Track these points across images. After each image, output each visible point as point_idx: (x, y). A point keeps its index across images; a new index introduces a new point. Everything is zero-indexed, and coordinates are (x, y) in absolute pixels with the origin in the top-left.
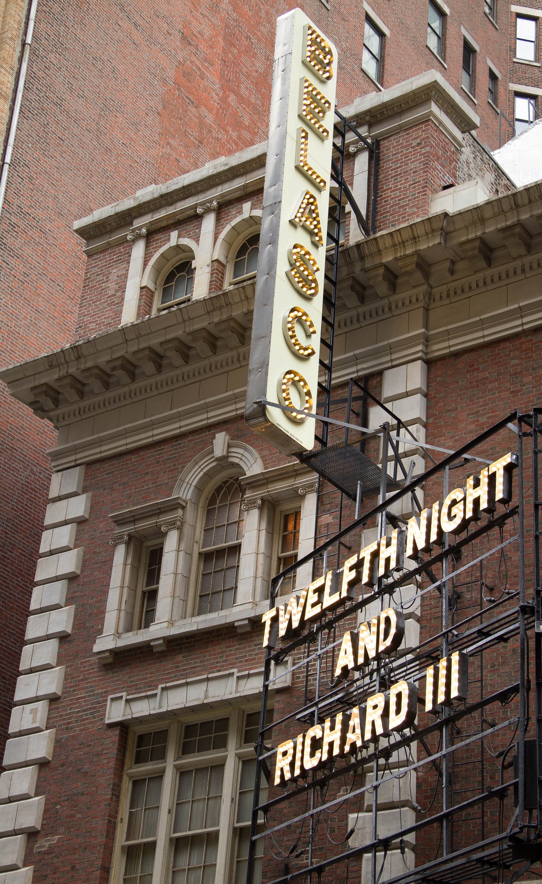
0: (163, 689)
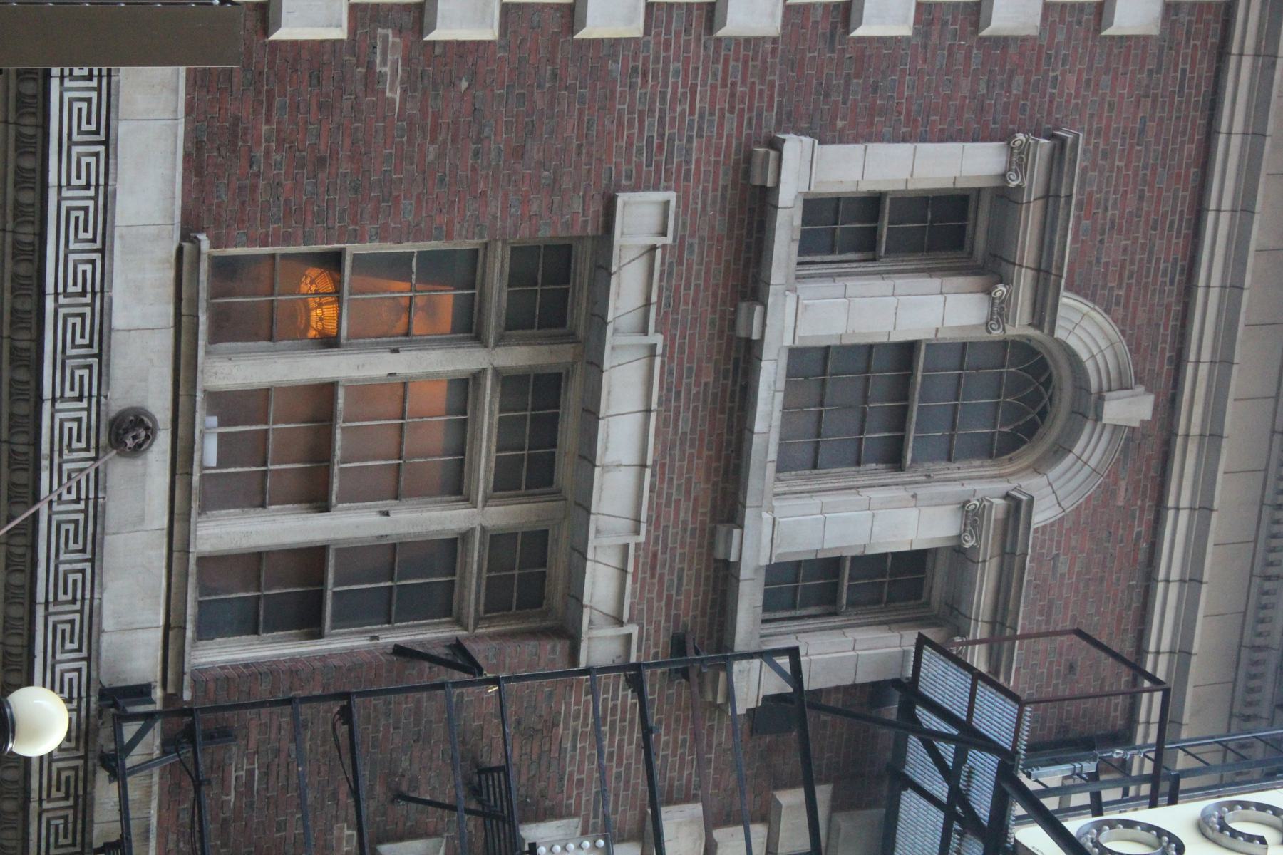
0: (653, 347)
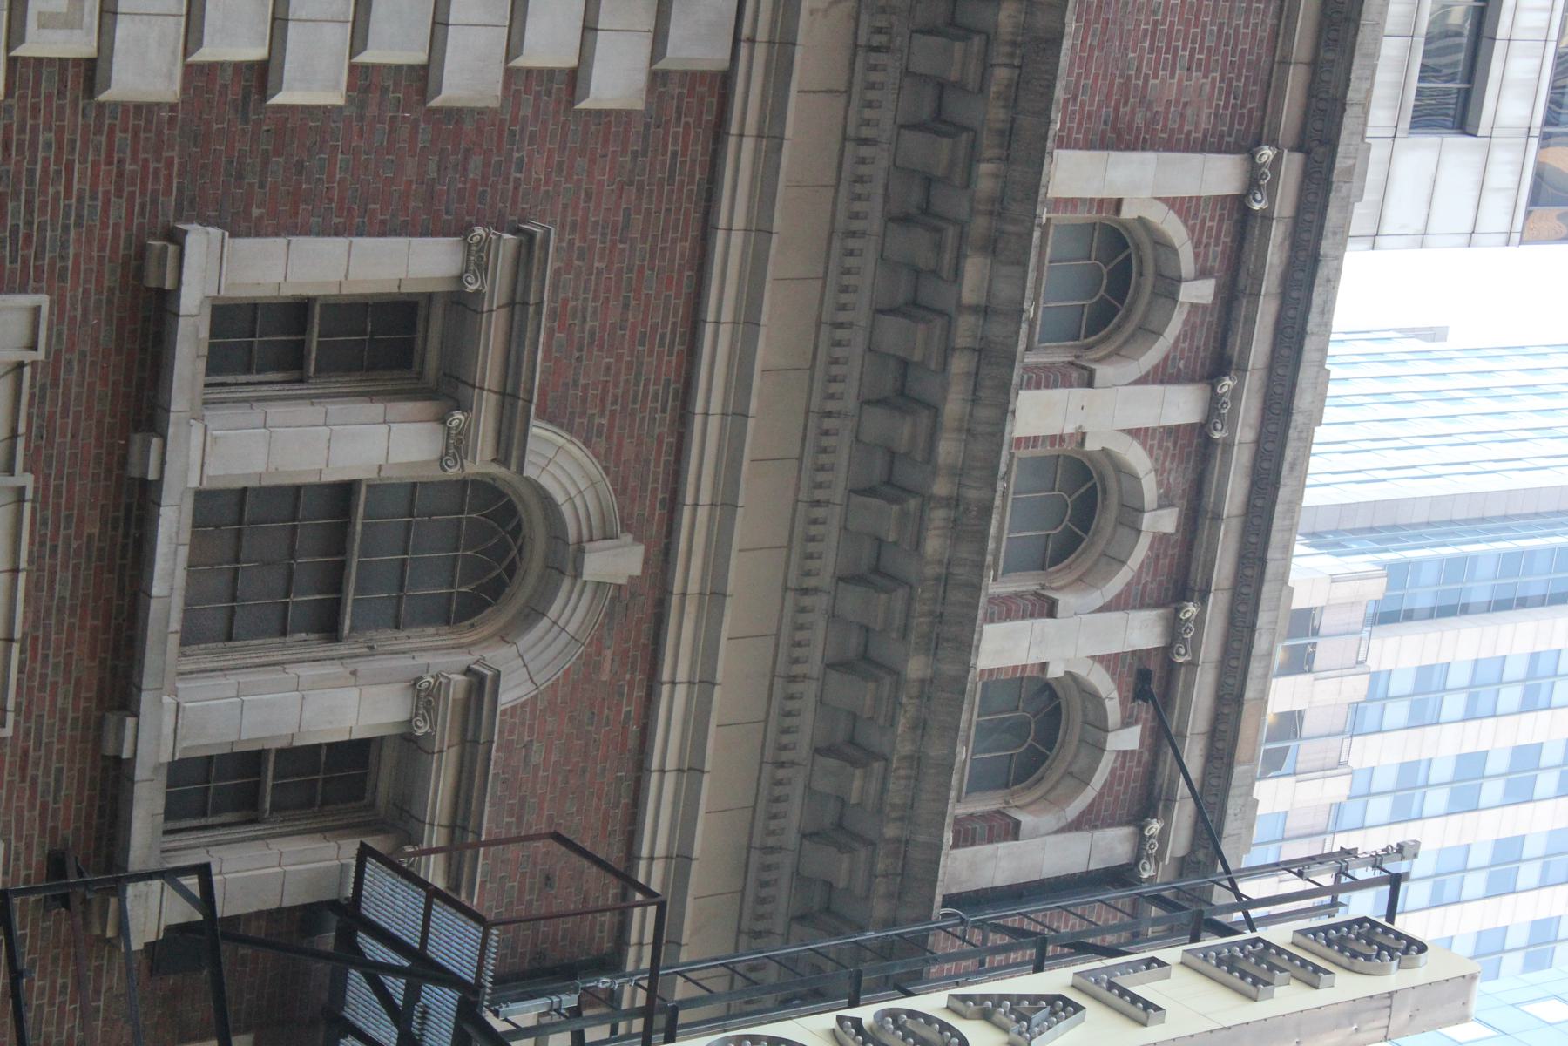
0: (21, 491)
